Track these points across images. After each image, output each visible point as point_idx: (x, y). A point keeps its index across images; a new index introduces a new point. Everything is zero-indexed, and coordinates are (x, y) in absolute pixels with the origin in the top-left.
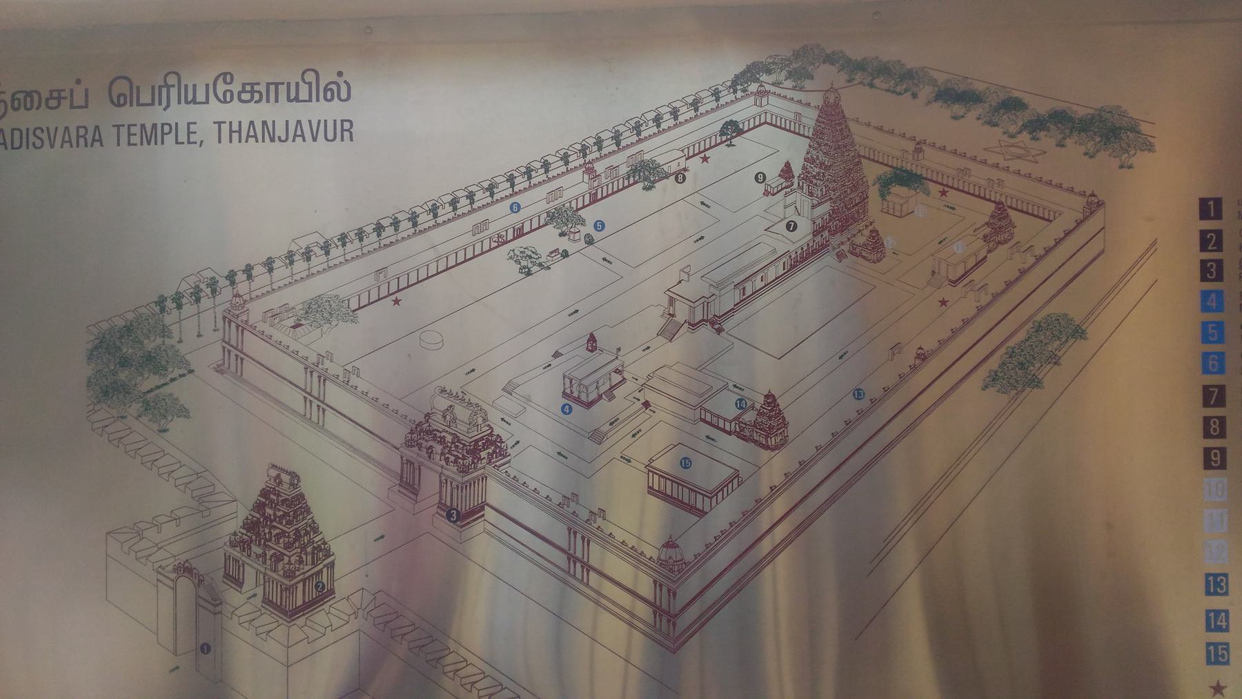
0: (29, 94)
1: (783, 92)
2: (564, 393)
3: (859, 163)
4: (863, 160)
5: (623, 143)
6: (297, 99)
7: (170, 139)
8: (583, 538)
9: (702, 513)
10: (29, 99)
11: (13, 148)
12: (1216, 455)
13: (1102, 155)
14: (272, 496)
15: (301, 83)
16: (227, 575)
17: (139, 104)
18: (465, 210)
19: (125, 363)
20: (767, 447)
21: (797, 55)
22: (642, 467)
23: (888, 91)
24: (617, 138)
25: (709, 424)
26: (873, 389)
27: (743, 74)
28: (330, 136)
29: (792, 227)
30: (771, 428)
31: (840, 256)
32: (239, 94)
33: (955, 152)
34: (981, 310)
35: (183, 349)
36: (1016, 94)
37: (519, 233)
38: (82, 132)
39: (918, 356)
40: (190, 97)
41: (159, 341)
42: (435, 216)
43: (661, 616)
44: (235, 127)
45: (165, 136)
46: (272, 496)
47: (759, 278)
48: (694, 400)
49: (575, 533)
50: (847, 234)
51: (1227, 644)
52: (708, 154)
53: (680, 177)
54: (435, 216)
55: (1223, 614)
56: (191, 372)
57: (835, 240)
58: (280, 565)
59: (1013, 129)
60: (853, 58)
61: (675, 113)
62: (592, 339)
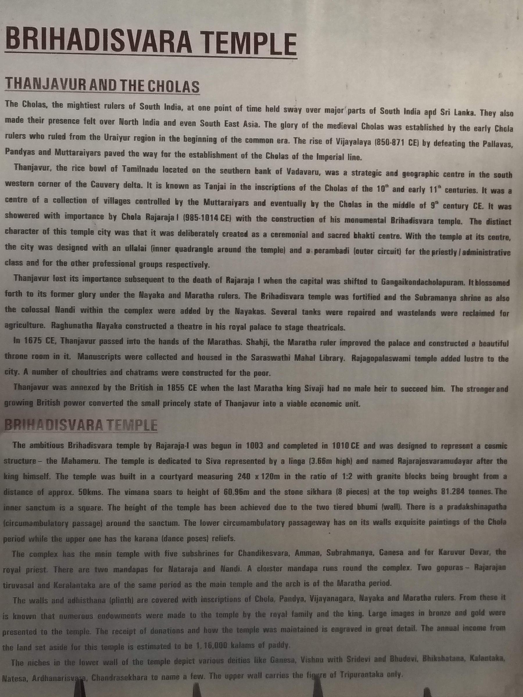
7: (264, 50)
38: (167, 37)
45: (259, 47)
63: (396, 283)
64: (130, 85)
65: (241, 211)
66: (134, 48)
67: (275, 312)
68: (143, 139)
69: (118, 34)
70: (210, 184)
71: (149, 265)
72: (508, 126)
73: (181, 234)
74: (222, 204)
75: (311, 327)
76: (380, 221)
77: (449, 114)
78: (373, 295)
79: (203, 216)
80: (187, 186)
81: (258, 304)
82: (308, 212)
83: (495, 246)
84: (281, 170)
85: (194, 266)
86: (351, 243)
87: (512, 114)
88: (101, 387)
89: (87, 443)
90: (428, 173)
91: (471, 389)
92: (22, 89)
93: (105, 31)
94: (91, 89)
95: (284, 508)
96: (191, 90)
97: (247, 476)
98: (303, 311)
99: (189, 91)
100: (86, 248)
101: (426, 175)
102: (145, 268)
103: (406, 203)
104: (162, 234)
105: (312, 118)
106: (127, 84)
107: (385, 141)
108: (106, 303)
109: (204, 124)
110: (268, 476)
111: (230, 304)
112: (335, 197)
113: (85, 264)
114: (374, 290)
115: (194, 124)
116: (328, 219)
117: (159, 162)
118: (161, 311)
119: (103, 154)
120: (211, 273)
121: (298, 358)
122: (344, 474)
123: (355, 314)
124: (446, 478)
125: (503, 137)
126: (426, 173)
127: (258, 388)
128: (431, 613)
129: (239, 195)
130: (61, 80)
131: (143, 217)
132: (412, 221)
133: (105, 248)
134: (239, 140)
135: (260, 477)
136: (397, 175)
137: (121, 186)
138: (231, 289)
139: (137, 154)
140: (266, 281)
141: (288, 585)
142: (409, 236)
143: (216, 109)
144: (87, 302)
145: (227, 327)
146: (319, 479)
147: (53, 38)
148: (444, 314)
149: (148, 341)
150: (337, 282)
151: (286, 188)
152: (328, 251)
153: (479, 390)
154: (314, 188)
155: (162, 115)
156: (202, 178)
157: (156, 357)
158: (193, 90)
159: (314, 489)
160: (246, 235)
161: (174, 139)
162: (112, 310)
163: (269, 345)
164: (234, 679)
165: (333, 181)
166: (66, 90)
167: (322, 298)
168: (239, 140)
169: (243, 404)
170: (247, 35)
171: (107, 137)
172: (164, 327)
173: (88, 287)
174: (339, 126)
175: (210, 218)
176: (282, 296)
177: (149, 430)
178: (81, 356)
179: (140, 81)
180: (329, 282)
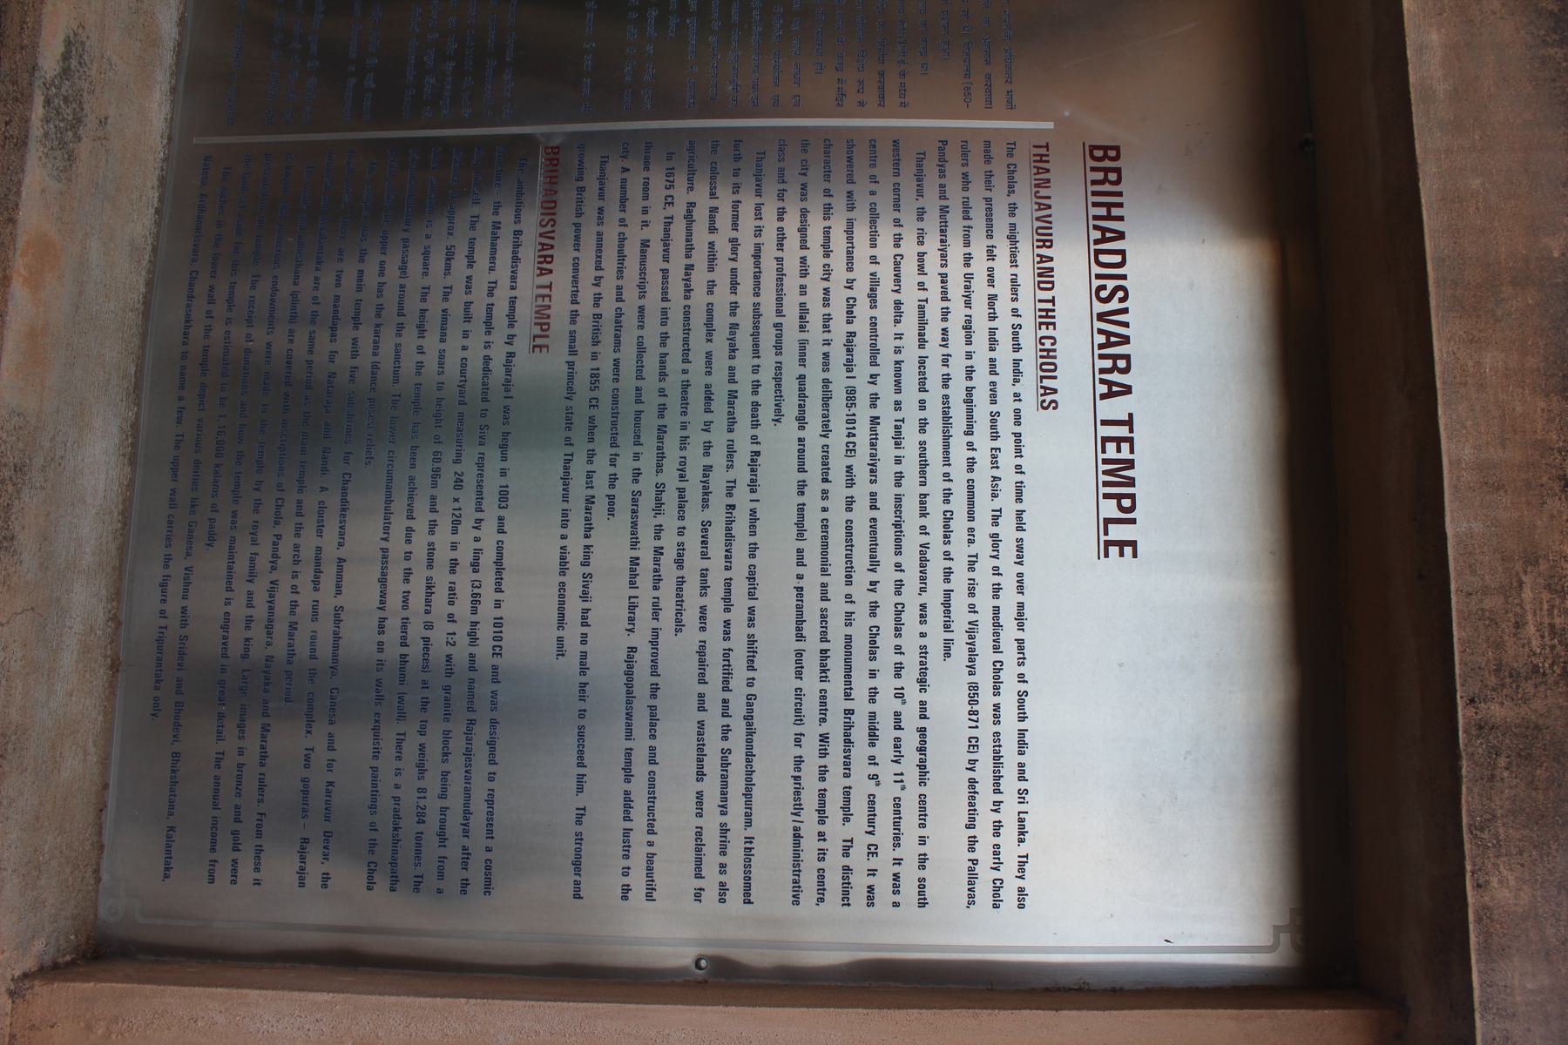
7: (1110, 509)
38: (1122, 364)
45: (1115, 501)
63: (749, 718)
64: (1047, 311)
65: (861, 473)
66: (1102, 317)
67: (706, 525)
68: (968, 327)
69: (1120, 294)
70: (903, 425)
71: (779, 336)
72: (1002, 901)
73: (826, 382)
74: (872, 444)
75: (681, 581)
76: (848, 691)
77: (1019, 803)
78: (730, 680)
79: (854, 415)
80: (898, 391)
81: (718, 499)
82: (862, 576)
83: (809, 880)
84: (926, 533)
85: (777, 402)
86: (812, 645)
87: (1021, 906)
88: (600, 273)
89: (520, 256)
90: (925, 768)
91: (579, 838)
92: (1033, 164)
93: (1124, 277)
94: (1038, 255)
95: (409, 541)
96: (1043, 398)
97: (459, 484)
98: (707, 570)
99: (1042, 395)
100: (804, 247)
101: (922, 766)
102: (774, 331)
103: (877, 733)
104: (826, 355)
105: (1008, 583)
106: (1049, 306)
107: (976, 698)
108: (722, 276)
109: (994, 417)
110: (457, 516)
111: (718, 457)
112: (886, 619)
113: (780, 246)
114: (738, 682)
115: (994, 402)
116: (850, 608)
117: (934, 351)
118: (709, 355)
119: (943, 270)
120: (766, 430)
121: (635, 561)
122: (455, 634)
123: (701, 652)
124: (443, 796)
125: (984, 890)
126: (925, 766)
127: (590, 500)
128: (240, 766)
129: (886, 469)
130: (1050, 216)
131: (851, 328)
132: (848, 742)
133: (804, 274)
134: (970, 470)
135: (457, 505)
136: (921, 718)
137: (897, 296)
138: (742, 459)
139: (945, 319)
140: (753, 512)
141: (296, 546)
142: (824, 738)
143: (1018, 435)
144: (724, 250)
145: (683, 453)
146: (450, 594)
147: (1109, 206)
148: (700, 795)
149: (665, 337)
150: (751, 622)
151: (898, 541)
152: (799, 608)
153: (578, 850)
154: (899, 585)
155: (1004, 354)
156: (911, 414)
157: (641, 349)
158: (1044, 401)
159: (434, 587)
160: (825, 480)
161: (970, 372)
162: (711, 285)
163: (655, 517)
164: (171, 468)
165: (911, 617)
166: (1034, 221)
167: (727, 599)
168: (970, 470)
169: (566, 479)
170: (1131, 482)
171: (968, 277)
172: (686, 361)
173: (746, 251)
174: (997, 625)
175: (851, 426)
176: (729, 536)
177: (534, 341)
178: (645, 244)
179: (1054, 324)
180: (751, 610)
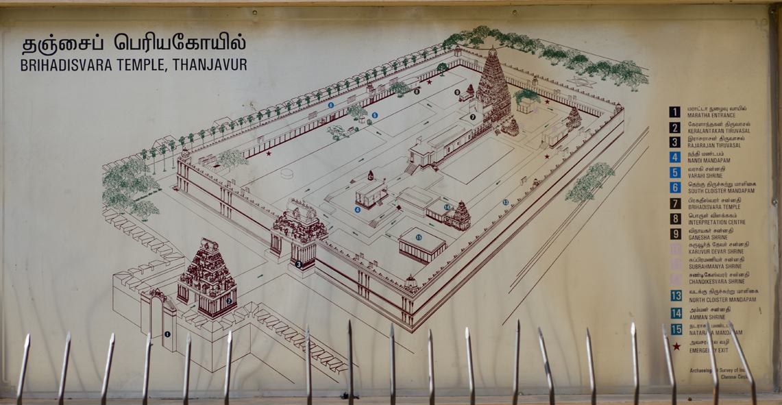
0: (69, 41)
1: (469, 50)
2: (356, 201)
3: (506, 86)
4: (508, 85)
5: (387, 74)
6: (217, 48)
7: (149, 67)
8: (366, 276)
9: (427, 263)
10: (69, 44)
11: (60, 70)
12: (676, 232)
13: (624, 85)
14: (204, 255)
15: (219, 39)
16: (179, 296)
17: (131, 49)
18: (305, 106)
19: (124, 185)
20: (460, 229)
21: (475, 31)
22: (396, 240)
23: (520, 50)
24: (384, 70)
25: (431, 217)
26: (513, 200)
27: (449, 40)
28: (235, 68)
29: (473, 117)
30: (462, 219)
31: (497, 133)
32: (187, 44)
33: (553, 82)
34: (565, 160)
35: (156, 178)
36: (582, 54)
37: (333, 119)
38: (100, 62)
39: (535, 183)
40: (160, 46)
41: (143, 173)
42: (289, 109)
43: (405, 315)
44: (184, 62)
46: (204, 255)
47: (456, 143)
48: (424, 206)
49: (362, 273)
50: (500, 122)
51: (681, 325)
52: (431, 79)
53: (417, 91)
54: (289, 109)
55: (679, 310)
56: (160, 190)
57: (496, 124)
58: (208, 291)
59: (581, 71)
60: (503, 33)
61: (414, 59)
62: (371, 173)
147: (43, 65)
